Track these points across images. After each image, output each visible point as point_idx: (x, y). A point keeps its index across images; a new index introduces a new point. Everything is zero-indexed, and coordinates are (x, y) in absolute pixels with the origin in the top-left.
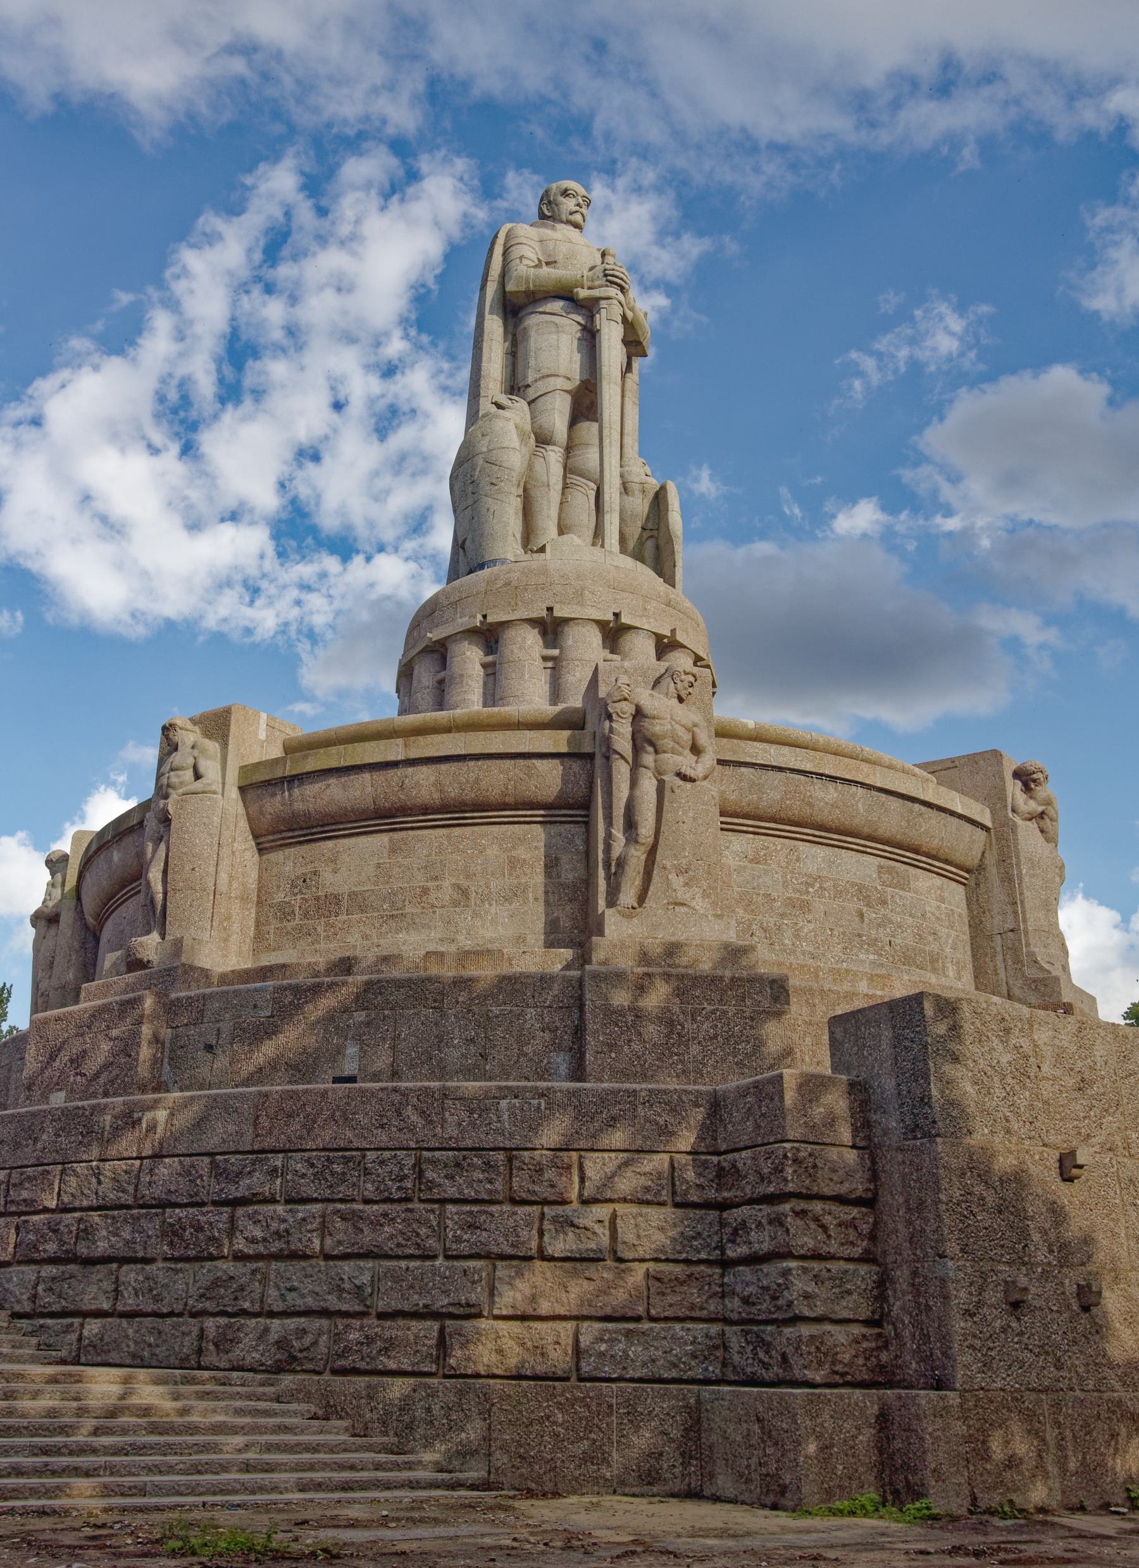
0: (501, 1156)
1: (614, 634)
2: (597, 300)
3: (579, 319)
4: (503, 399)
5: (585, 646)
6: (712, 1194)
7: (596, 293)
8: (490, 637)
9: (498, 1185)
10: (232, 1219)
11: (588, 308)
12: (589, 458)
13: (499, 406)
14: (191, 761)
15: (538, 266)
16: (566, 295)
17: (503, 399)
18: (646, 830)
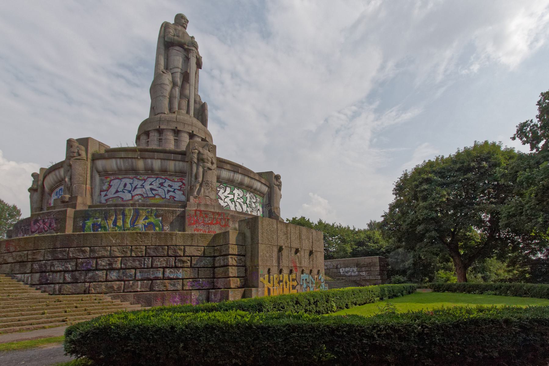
0: (166, 247)
1: (192, 136)
2: (190, 50)
3: (185, 54)
4: (165, 71)
5: (185, 138)
6: (213, 255)
7: (190, 48)
8: (160, 131)
9: (166, 253)
10: (97, 262)
11: (187, 51)
12: (187, 92)
13: (163, 72)
14: (77, 151)
15: (174, 36)
16: (181, 45)
17: (165, 71)
18: (200, 179)
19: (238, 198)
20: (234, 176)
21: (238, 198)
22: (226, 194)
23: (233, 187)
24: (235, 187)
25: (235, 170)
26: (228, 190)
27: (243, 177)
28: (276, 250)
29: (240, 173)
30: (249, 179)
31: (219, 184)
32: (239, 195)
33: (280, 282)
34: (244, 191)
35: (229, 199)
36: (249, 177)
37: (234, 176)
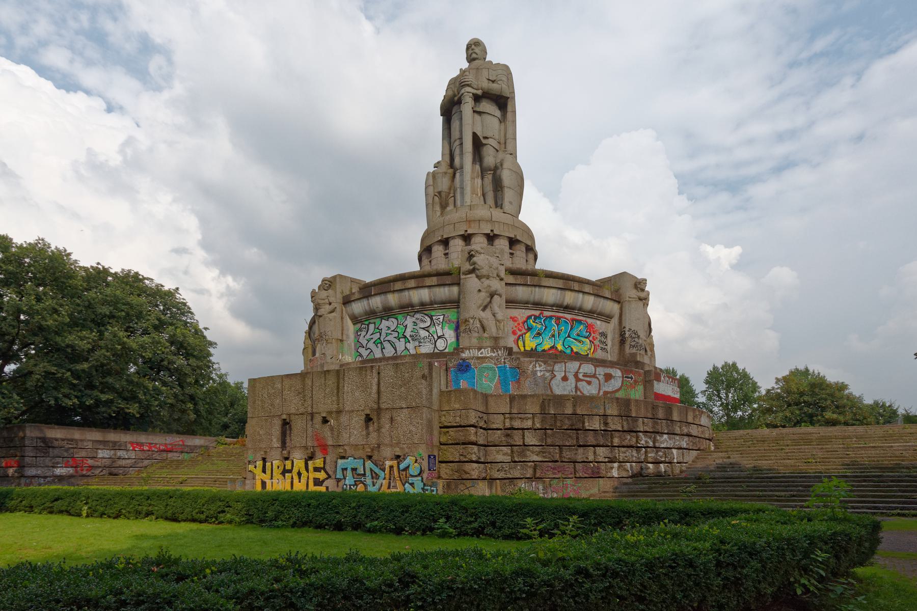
19: (387, 335)
20: (369, 304)
21: (387, 335)
22: (368, 337)
23: (378, 321)
24: (382, 318)
25: (367, 294)
26: (372, 327)
27: (383, 296)
28: (277, 423)
29: (375, 295)
30: (396, 295)
31: (359, 325)
32: (389, 328)
33: (284, 472)
34: (400, 317)
35: (373, 341)
36: (394, 291)
37: (369, 304)
